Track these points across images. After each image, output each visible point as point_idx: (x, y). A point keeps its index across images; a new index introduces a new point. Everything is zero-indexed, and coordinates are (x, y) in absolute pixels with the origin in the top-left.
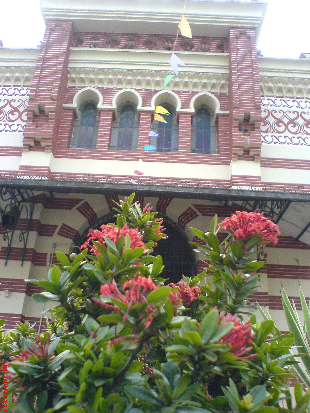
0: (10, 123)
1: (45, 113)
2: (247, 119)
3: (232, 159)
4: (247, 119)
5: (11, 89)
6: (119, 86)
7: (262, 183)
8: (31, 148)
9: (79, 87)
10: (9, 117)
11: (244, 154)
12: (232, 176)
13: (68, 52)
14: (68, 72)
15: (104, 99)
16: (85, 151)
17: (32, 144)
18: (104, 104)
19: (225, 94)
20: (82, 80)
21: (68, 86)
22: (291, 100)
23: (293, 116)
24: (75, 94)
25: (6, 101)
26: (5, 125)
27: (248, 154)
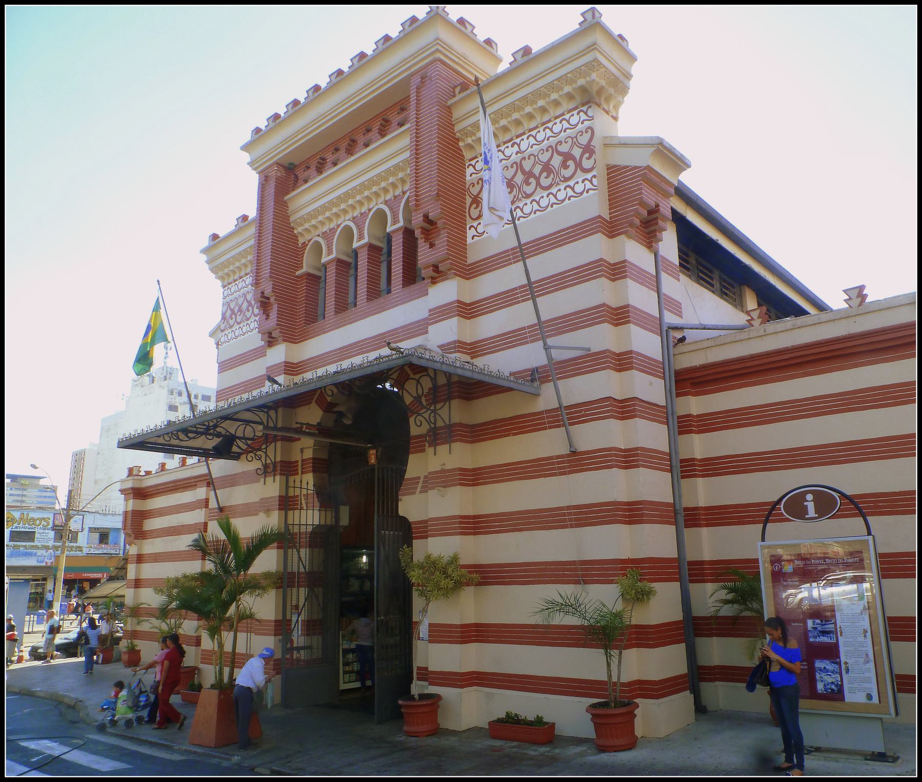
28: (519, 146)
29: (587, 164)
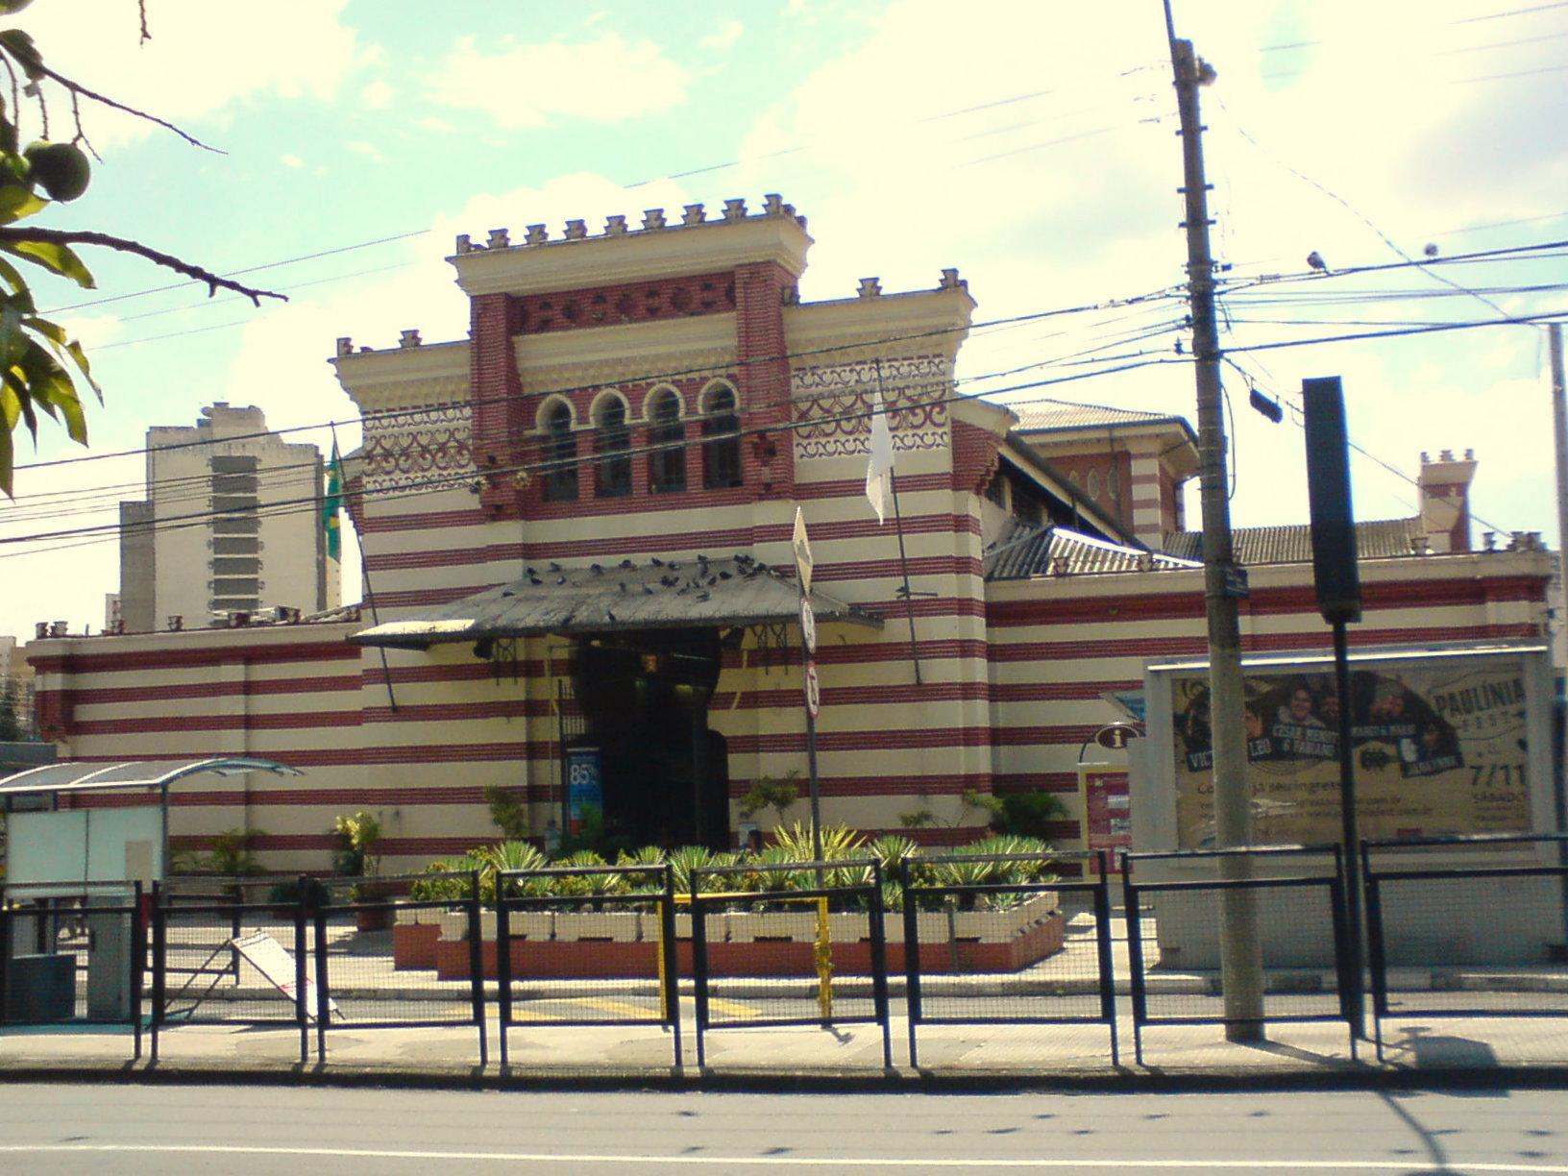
22: (848, 369)
28: (859, 373)
29: (938, 418)
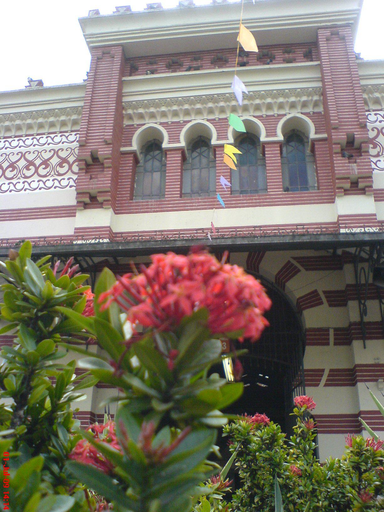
0: (59, 178)
1: (99, 161)
2: (351, 142)
3: (337, 194)
4: (351, 142)
5: (57, 136)
6: (187, 119)
7: (379, 222)
8: (86, 206)
9: (138, 125)
10: (24, 173)
11: (351, 187)
12: (339, 216)
13: (121, 84)
14: (123, 108)
15: (169, 136)
16: (152, 202)
17: (87, 200)
18: (170, 142)
19: (320, 113)
20: (141, 116)
21: (124, 126)
23: (46, 156)
24: (133, 134)
25: (53, 152)
26: (53, 180)
27: (357, 186)
